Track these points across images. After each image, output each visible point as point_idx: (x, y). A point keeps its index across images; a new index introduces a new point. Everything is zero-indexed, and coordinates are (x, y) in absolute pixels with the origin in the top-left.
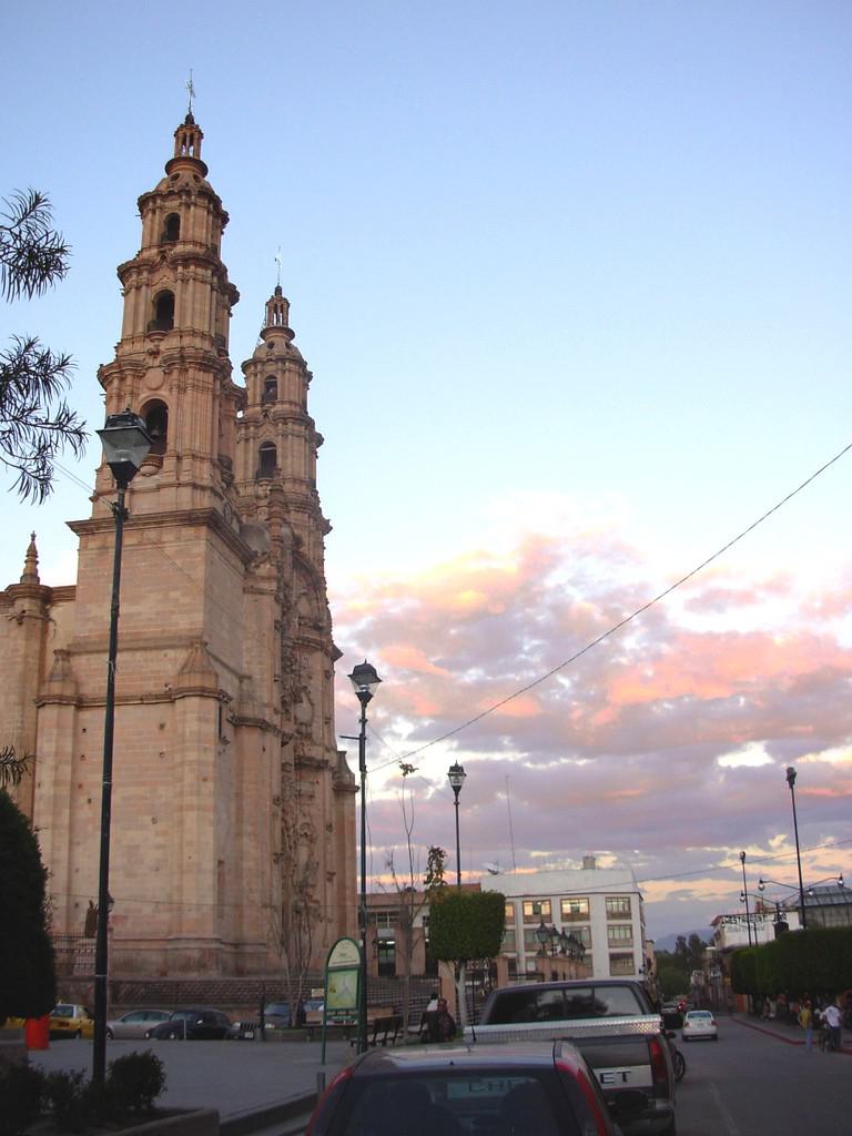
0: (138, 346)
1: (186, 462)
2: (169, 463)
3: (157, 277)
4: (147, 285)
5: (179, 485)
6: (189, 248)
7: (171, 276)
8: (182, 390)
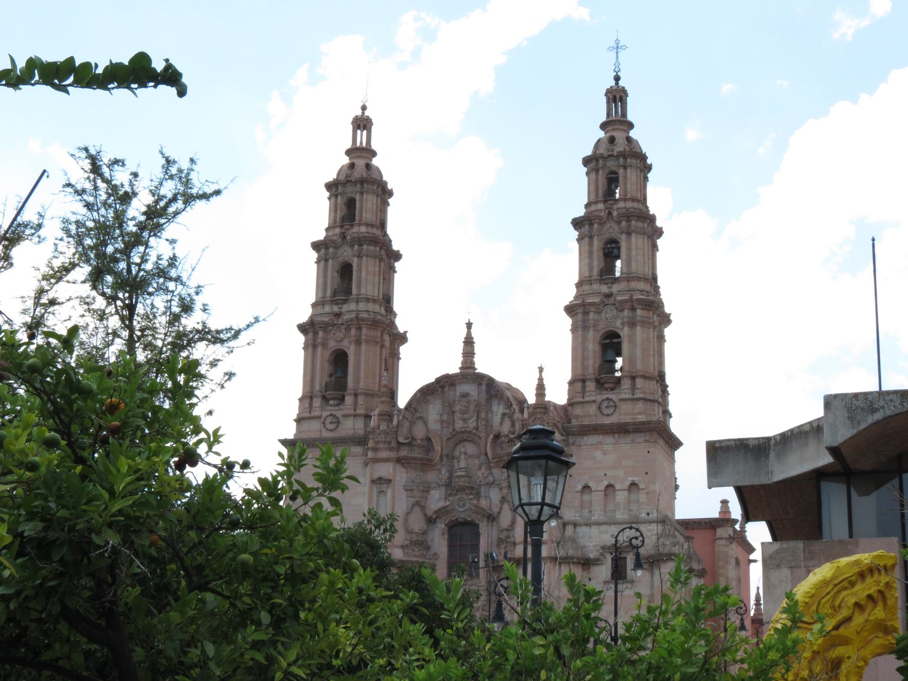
0: (327, 309)
1: (361, 399)
2: (349, 400)
3: (341, 251)
4: (333, 259)
5: (355, 416)
6: (363, 229)
7: (350, 252)
8: (358, 343)
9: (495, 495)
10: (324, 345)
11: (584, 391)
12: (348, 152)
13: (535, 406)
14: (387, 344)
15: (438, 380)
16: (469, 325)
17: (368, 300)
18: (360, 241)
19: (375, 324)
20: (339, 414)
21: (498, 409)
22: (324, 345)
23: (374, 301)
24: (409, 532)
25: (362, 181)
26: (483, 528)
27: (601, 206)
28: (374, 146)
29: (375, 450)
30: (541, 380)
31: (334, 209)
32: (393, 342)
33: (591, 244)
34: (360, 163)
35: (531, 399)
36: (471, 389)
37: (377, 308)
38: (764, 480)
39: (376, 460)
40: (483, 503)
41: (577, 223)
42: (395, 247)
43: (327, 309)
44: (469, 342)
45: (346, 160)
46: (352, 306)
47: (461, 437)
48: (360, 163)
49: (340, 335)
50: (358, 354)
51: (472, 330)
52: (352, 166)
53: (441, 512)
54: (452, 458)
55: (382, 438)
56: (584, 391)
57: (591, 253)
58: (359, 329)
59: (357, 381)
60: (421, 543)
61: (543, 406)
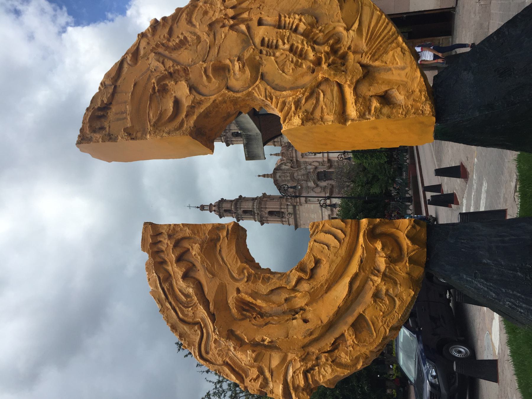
0: (256, 217)
2: (283, 210)
6: (233, 207)
8: (266, 208)
9: (309, 167)
10: (267, 218)
11: (278, 142)
12: (211, 212)
13: (282, 156)
14: (266, 199)
15: (276, 185)
16: (259, 176)
17: (253, 205)
18: (236, 208)
19: (260, 203)
20: (287, 213)
21: (284, 167)
22: (267, 218)
23: (253, 204)
24: (321, 192)
25: (219, 208)
26: (319, 170)
27: (222, 138)
28: (209, 204)
29: (297, 203)
30: (274, 155)
31: (227, 216)
32: (266, 198)
33: (234, 141)
34: (214, 208)
35: (280, 157)
36: (278, 175)
37: (256, 203)
38: (260, 136)
39: (300, 203)
40: (312, 171)
41: (228, 145)
42: (238, 197)
43: (256, 217)
44: (264, 176)
45: (213, 212)
46: (255, 210)
47: (293, 178)
48: (214, 208)
49: (264, 213)
50: (269, 208)
51: (261, 175)
52: (215, 211)
53: (315, 183)
54: (299, 180)
55: (293, 201)
56: (278, 142)
57: (236, 141)
58: (262, 208)
59: (277, 208)
60: (324, 189)
61: (282, 154)
